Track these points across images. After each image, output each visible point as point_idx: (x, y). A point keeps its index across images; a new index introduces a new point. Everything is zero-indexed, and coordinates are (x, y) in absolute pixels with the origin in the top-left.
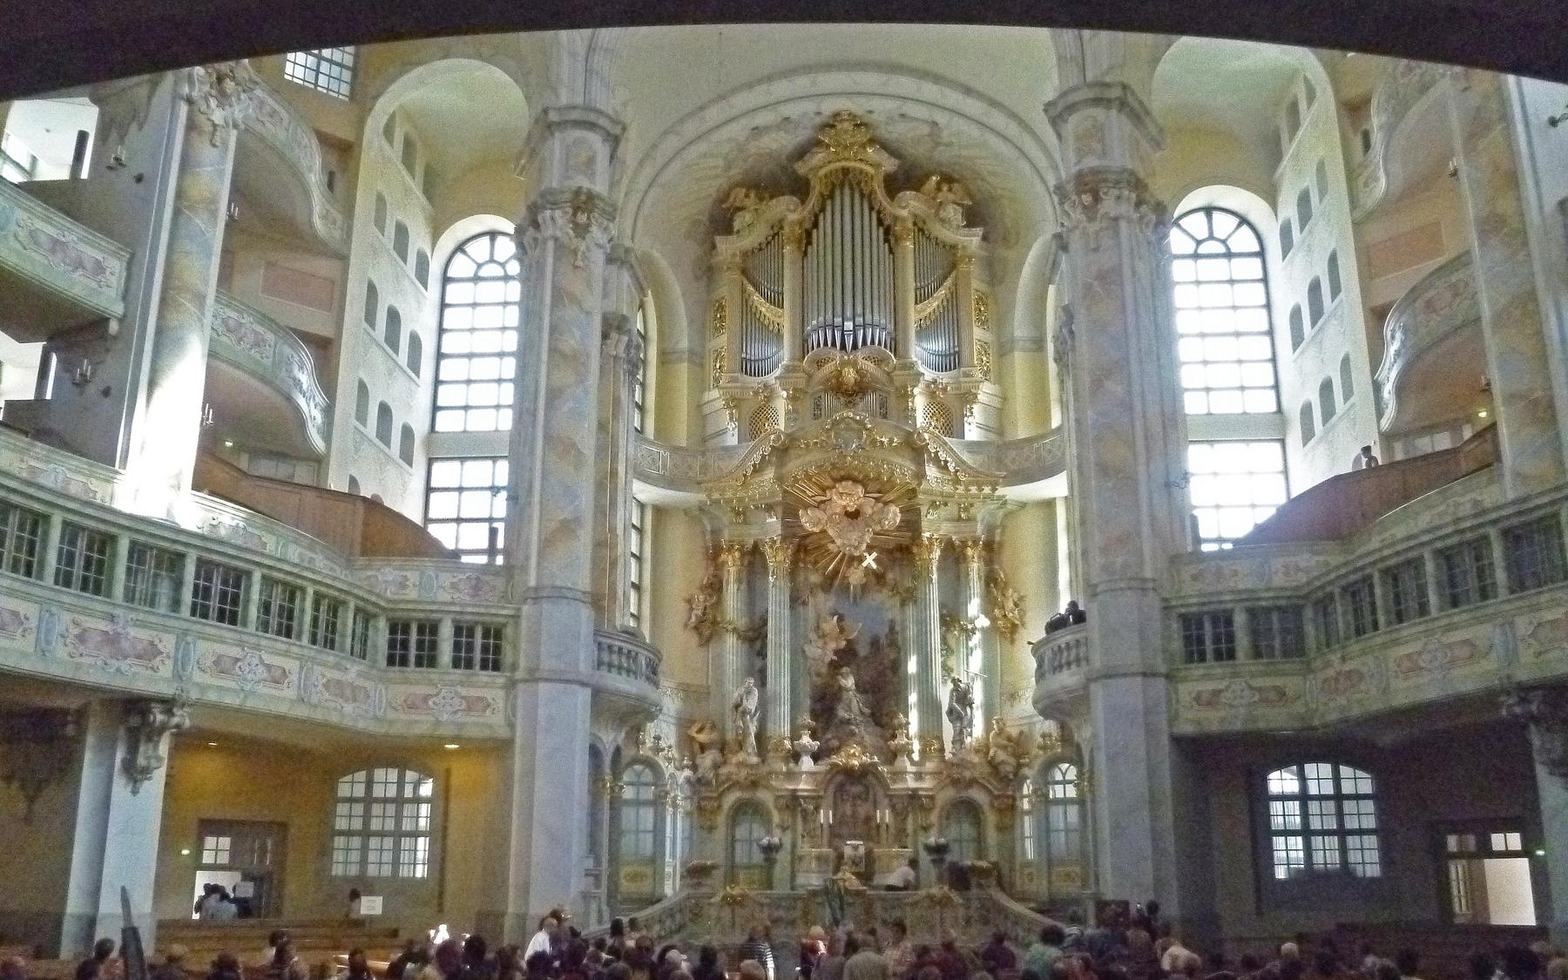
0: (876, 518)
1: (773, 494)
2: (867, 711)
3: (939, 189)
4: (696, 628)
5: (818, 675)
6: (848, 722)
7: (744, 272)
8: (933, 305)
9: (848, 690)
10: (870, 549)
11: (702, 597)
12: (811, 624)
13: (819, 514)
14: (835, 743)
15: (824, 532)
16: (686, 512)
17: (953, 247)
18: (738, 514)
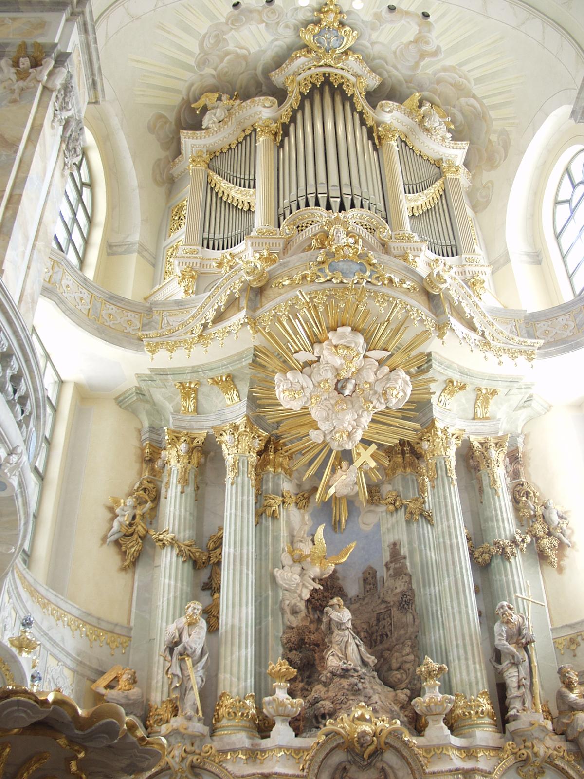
0: (379, 389)
1: (240, 357)
2: (372, 660)
3: (420, 106)
4: (117, 543)
5: (295, 612)
6: (345, 673)
7: (209, 167)
8: (422, 200)
9: (340, 625)
10: (366, 442)
11: (130, 501)
12: (284, 544)
13: (302, 379)
14: (327, 705)
15: (305, 412)
16: (121, 401)
17: (437, 164)
18: (187, 396)
